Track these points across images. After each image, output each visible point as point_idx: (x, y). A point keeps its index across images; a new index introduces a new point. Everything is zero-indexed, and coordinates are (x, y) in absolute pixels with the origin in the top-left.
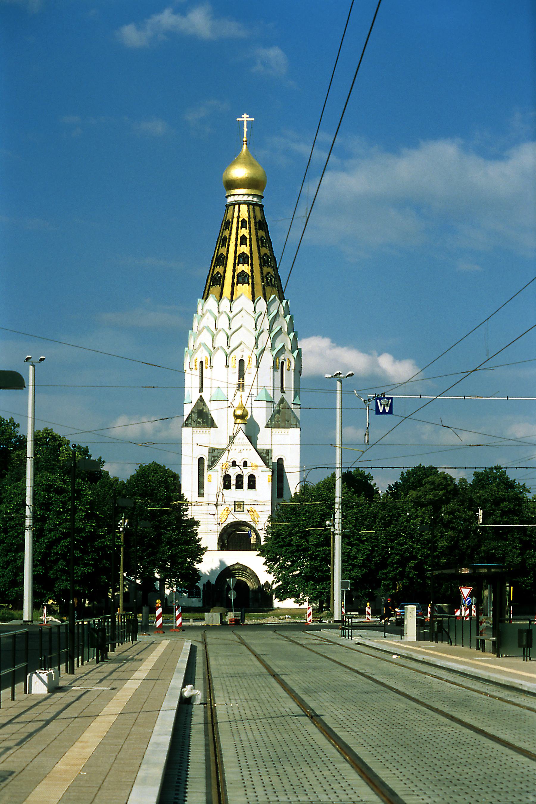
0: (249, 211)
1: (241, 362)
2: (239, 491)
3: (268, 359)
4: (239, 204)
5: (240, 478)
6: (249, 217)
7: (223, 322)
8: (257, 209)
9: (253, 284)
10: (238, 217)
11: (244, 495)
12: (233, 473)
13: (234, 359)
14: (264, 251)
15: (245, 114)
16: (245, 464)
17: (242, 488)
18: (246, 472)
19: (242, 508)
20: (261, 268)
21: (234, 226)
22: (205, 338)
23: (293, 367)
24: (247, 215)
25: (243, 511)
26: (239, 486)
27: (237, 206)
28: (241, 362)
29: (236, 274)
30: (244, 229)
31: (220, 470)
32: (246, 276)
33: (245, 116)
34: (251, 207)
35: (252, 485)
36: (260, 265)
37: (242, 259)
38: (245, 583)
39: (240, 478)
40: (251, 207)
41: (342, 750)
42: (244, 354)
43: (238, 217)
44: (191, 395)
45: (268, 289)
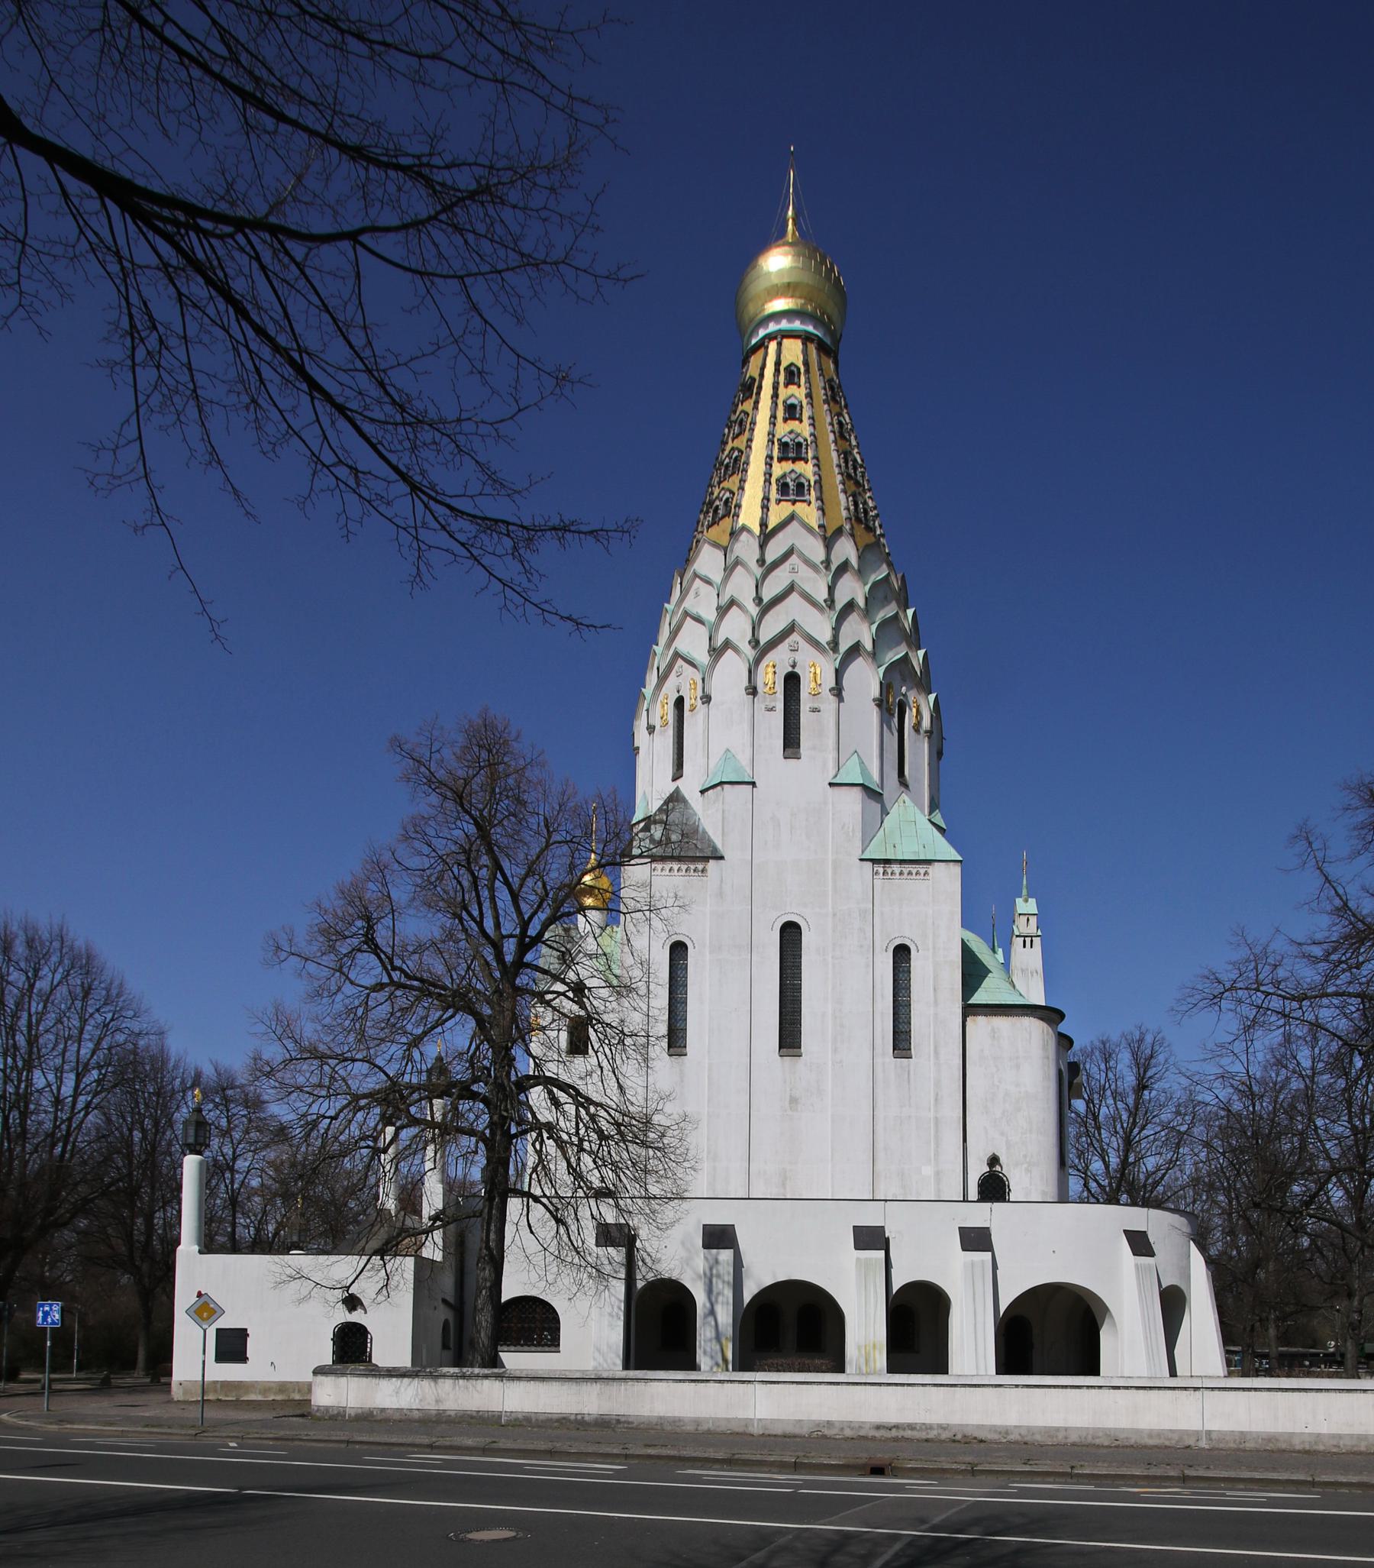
0: (805, 352)
1: (792, 681)
3: (865, 679)
6: (806, 363)
7: (742, 586)
10: (778, 364)
13: (771, 670)
22: (693, 642)
23: (926, 723)
27: (773, 346)
28: (792, 681)
30: (793, 389)
37: (792, 412)
41: (896, 1439)
42: (799, 657)
44: (651, 787)
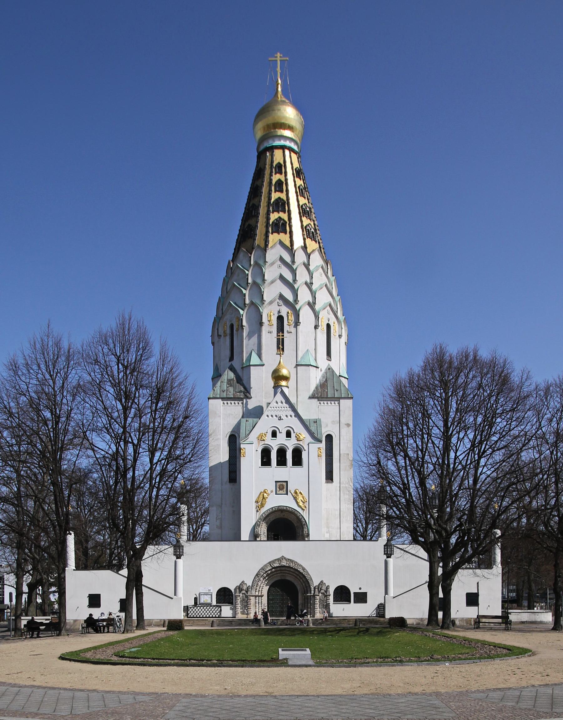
1: (280, 319)
2: (282, 469)
4: (272, 149)
5: (282, 452)
8: (294, 156)
9: (291, 232)
11: (288, 473)
12: (274, 445)
14: (303, 201)
15: (279, 54)
16: (288, 434)
17: (286, 465)
18: (290, 445)
19: (285, 489)
20: (301, 217)
21: (267, 172)
24: (282, 159)
25: (287, 494)
26: (282, 462)
29: (271, 223)
31: (255, 441)
32: (282, 224)
33: (279, 54)
34: (287, 152)
35: (297, 461)
36: (300, 213)
38: (293, 584)
39: (282, 452)
40: (287, 152)
43: (272, 162)
45: (308, 241)
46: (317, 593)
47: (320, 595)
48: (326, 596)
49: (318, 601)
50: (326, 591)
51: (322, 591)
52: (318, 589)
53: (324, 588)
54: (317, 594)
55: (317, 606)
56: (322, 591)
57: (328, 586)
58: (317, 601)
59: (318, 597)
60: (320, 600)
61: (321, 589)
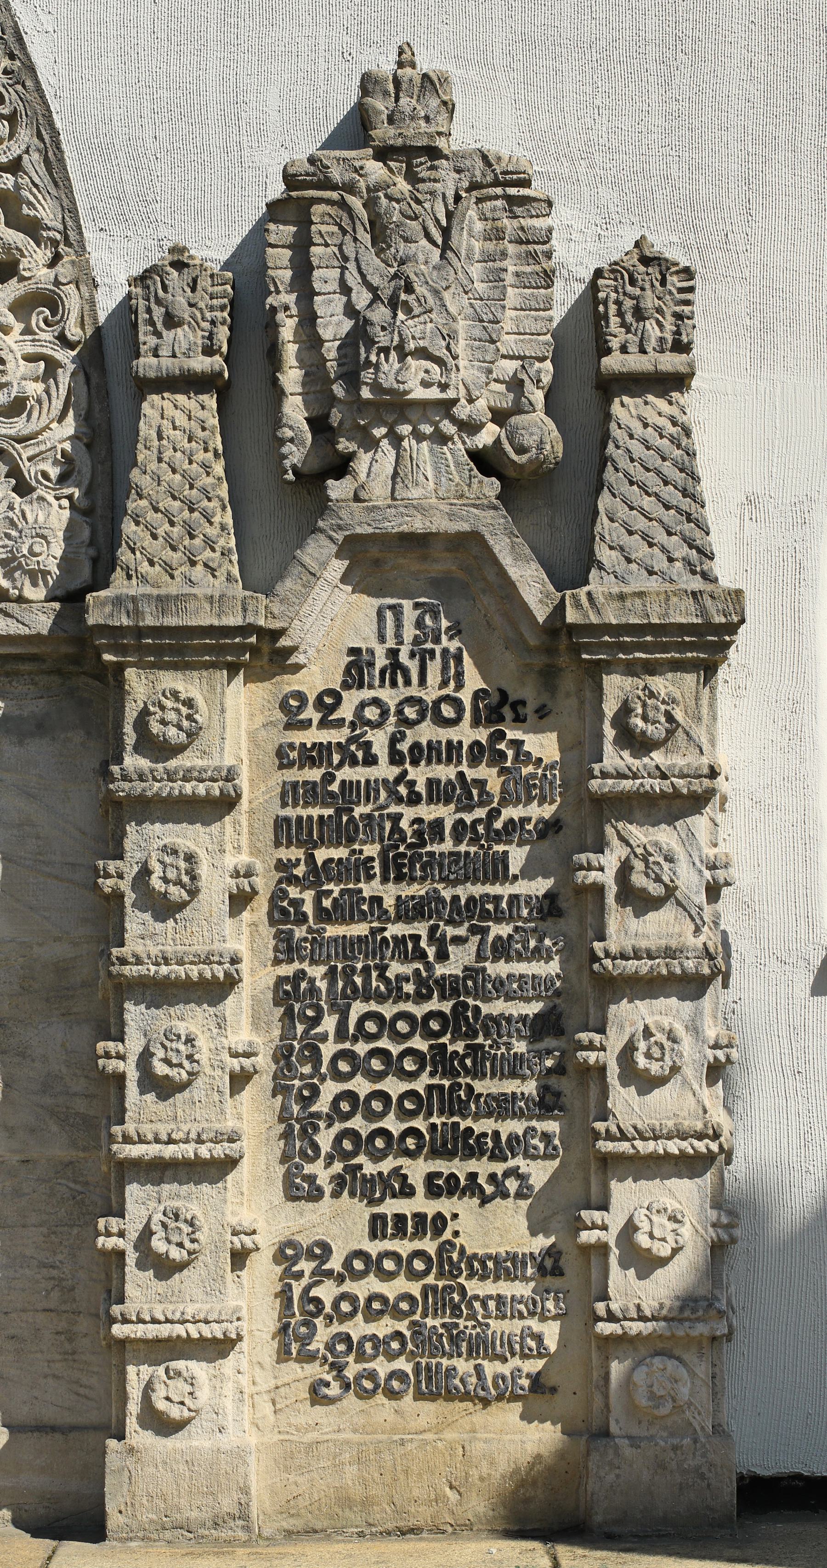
46: (182, 556)
47: (331, 619)
48: (558, 665)
49: (230, 851)
50: (554, 494)
51: (415, 484)
52: (240, 388)
53: (477, 349)
54: (212, 593)
55: (213, 1070)
56: (415, 484)
57: (651, 277)
58: (213, 892)
59: (233, 725)
60: (321, 815)
61: (358, 406)
